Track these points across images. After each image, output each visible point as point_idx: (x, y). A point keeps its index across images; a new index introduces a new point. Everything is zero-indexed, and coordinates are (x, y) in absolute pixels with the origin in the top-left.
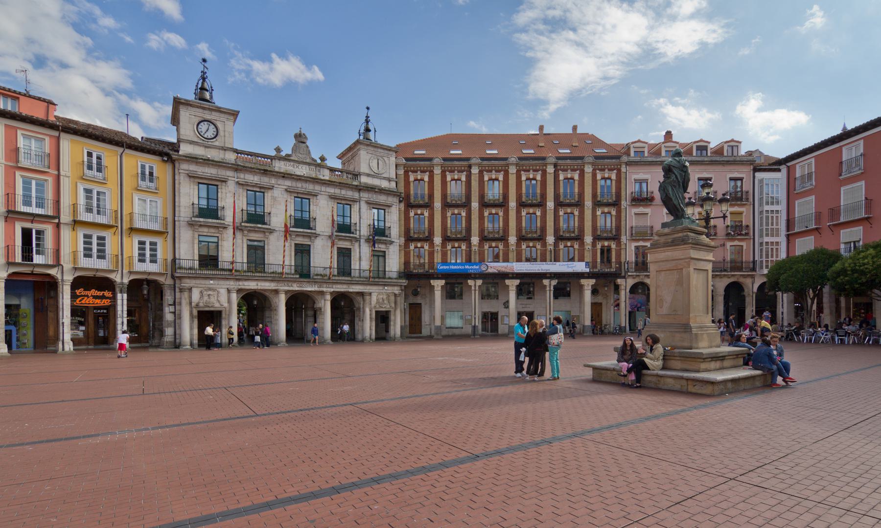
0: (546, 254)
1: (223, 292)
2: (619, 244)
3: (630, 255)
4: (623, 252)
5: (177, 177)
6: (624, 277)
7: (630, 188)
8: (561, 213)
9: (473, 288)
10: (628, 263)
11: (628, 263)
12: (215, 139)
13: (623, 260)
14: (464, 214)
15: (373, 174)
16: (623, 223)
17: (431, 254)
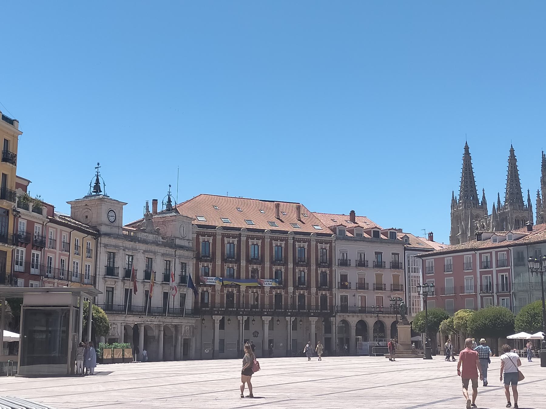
0: (288, 299)
1: (119, 325)
2: (331, 294)
3: (338, 302)
4: (334, 299)
5: (99, 249)
6: (335, 316)
7: (338, 256)
8: (297, 270)
9: (241, 322)
10: (337, 307)
11: (337, 307)
12: (115, 222)
13: (334, 305)
14: (235, 268)
15: (181, 237)
16: (334, 279)
17: (213, 296)
